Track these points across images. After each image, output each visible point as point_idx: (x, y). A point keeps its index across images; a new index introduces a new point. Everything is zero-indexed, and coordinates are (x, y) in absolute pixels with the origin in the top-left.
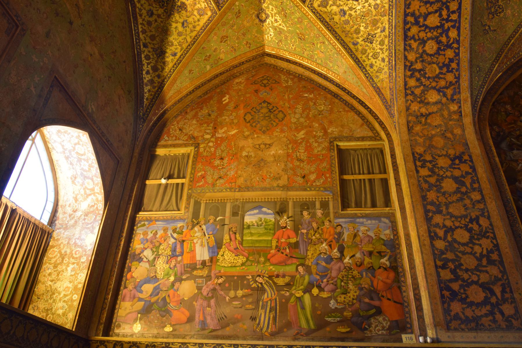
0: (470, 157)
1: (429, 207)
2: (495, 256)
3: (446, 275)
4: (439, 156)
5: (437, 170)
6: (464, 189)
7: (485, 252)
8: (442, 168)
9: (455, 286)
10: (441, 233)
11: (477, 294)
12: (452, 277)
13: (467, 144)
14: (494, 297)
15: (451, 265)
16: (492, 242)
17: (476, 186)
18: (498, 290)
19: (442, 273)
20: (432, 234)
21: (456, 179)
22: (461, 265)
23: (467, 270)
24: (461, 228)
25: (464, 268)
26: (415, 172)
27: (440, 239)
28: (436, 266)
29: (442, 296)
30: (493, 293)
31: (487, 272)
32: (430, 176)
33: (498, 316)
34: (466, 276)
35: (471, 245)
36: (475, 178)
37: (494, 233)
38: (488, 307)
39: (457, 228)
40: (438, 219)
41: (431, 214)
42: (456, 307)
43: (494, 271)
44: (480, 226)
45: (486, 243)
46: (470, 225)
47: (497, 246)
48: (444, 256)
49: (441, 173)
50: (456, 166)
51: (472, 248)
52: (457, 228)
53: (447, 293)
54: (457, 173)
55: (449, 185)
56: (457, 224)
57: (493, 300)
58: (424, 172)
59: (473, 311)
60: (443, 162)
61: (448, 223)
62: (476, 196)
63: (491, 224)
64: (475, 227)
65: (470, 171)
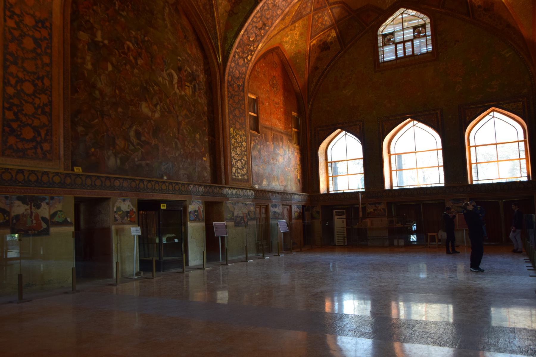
0: (51, 25)
1: (8, 57)
2: (47, 109)
3: (10, 115)
4: (27, 14)
5: (22, 26)
6: (39, 51)
7: (41, 105)
8: (27, 25)
9: (15, 125)
10: (13, 81)
11: (28, 133)
12: (14, 118)
13: (51, 14)
14: (40, 137)
15: (15, 109)
16: (48, 98)
17: (48, 51)
18: (43, 133)
19: (7, 113)
20: (6, 81)
21: (35, 40)
22: (23, 110)
23: (26, 115)
24: (29, 81)
25: (24, 112)
26: (3, 20)
27: (11, 86)
28: (4, 107)
29: (4, 131)
30: (39, 134)
31: (39, 119)
32: (15, 29)
33: (39, 151)
34: (24, 119)
35: (33, 97)
36: (50, 45)
37: (51, 92)
38: (34, 144)
39: (26, 80)
40: (13, 69)
41: (8, 63)
42: (12, 140)
43: (44, 119)
44: (43, 84)
45: (44, 98)
46: (37, 82)
47: (51, 102)
48: (11, 101)
49: (25, 30)
50: (38, 29)
51: (34, 99)
52: (26, 80)
53: (7, 129)
54: (37, 35)
55: (29, 43)
56: (27, 78)
57: (39, 139)
58: (11, 23)
59: (23, 145)
60: (28, 20)
61: (20, 75)
62: (46, 60)
63: (51, 85)
64: (40, 84)
65: (48, 37)
